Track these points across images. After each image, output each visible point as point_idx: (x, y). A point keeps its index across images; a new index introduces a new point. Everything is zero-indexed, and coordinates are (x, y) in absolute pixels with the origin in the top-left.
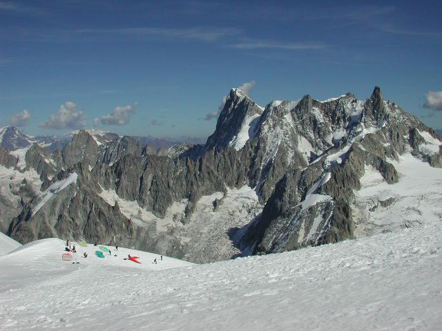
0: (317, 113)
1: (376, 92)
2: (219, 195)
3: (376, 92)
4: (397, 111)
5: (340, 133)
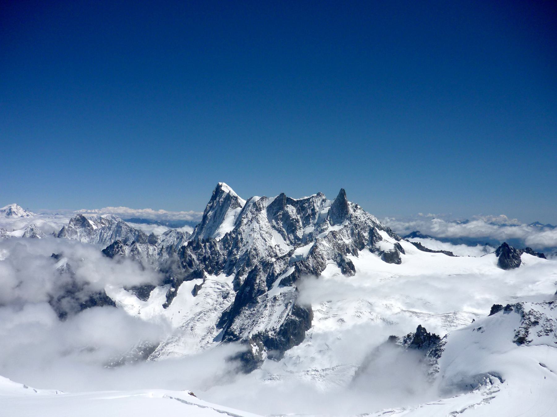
0: (291, 210)
1: (342, 193)
2: (199, 282)
3: (342, 193)
4: (359, 211)
5: (310, 229)
